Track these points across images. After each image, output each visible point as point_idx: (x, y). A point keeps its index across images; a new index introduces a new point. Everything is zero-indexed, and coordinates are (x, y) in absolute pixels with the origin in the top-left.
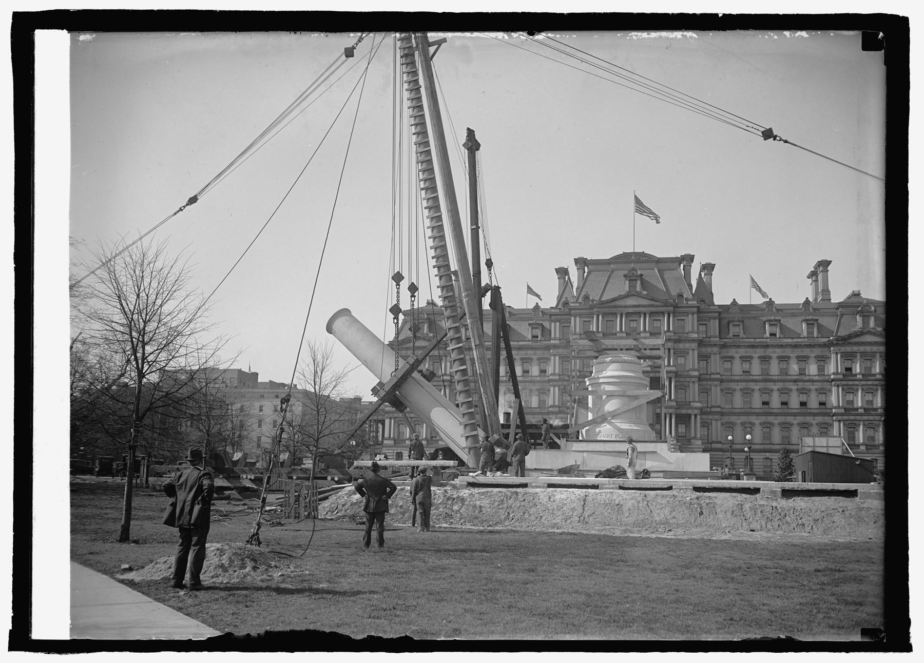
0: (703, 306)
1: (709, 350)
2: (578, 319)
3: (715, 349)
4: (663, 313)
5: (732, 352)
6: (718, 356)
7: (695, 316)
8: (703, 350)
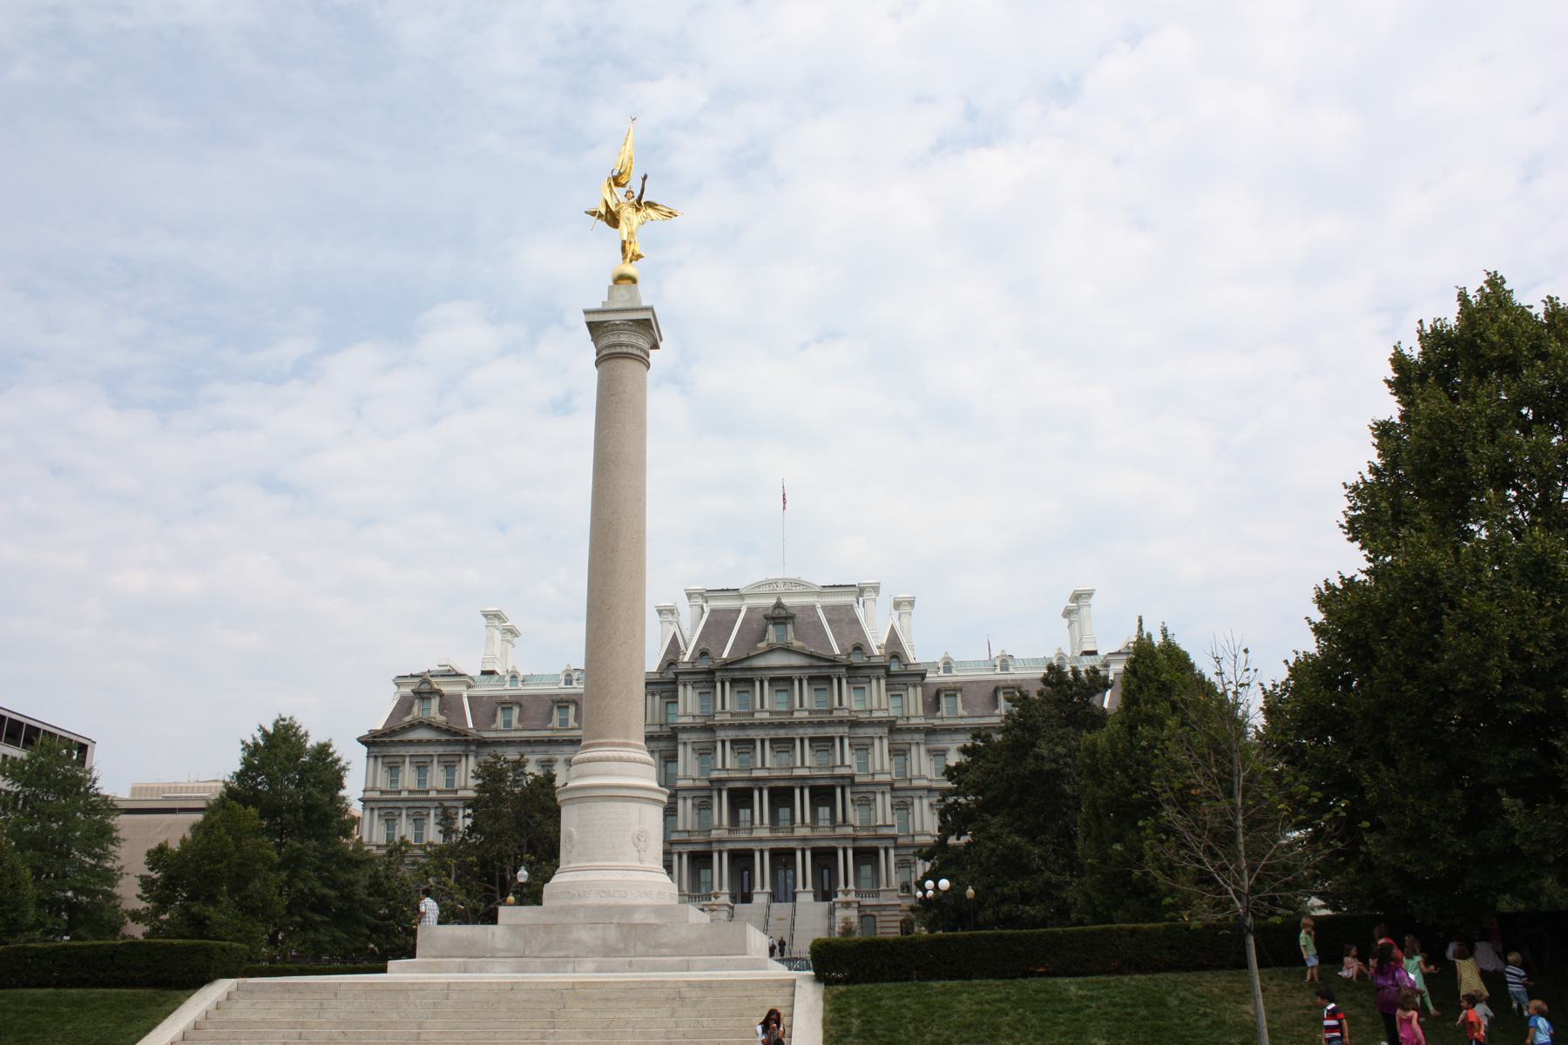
0: (894, 667)
1: (907, 738)
2: (689, 688)
3: (919, 737)
4: (751, 682)
6: (923, 749)
7: (883, 682)
8: (898, 738)
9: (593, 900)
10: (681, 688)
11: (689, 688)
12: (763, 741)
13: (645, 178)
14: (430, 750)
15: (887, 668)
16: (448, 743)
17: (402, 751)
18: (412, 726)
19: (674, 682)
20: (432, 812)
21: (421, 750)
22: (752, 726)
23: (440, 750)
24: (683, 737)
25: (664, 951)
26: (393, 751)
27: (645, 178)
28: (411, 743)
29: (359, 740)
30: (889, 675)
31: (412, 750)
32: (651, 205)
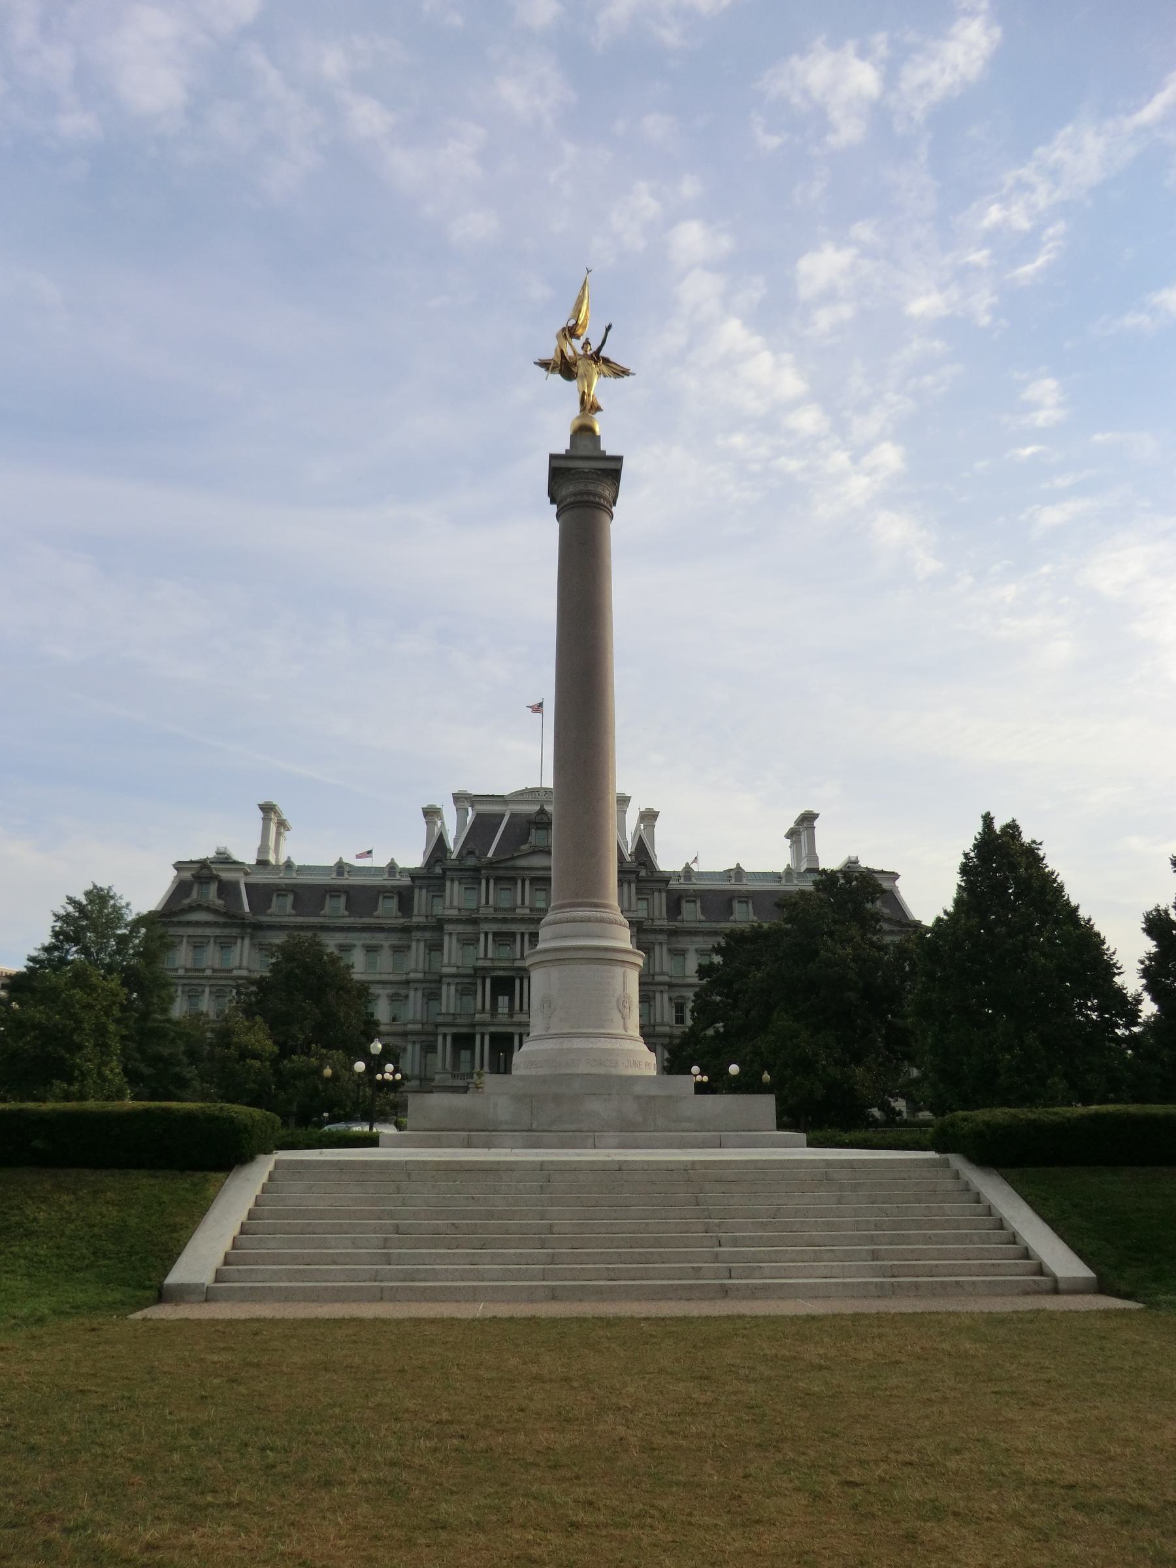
1: (652, 937)
2: (456, 883)
3: (662, 938)
4: (513, 880)
5: (683, 943)
6: (665, 948)
7: (633, 886)
9: (583, 1069)
10: (448, 884)
11: (456, 883)
12: (522, 934)
13: (608, 329)
14: (208, 931)
16: (225, 925)
17: (181, 931)
18: (192, 909)
19: (443, 877)
20: (207, 990)
21: (199, 931)
22: (514, 920)
23: (218, 931)
24: (448, 927)
25: (687, 1125)
27: (608, 329)
28: (189, 924)
29: (817, 815)
30: (639, 880)
31: (191, 931)
32: (606, 361)
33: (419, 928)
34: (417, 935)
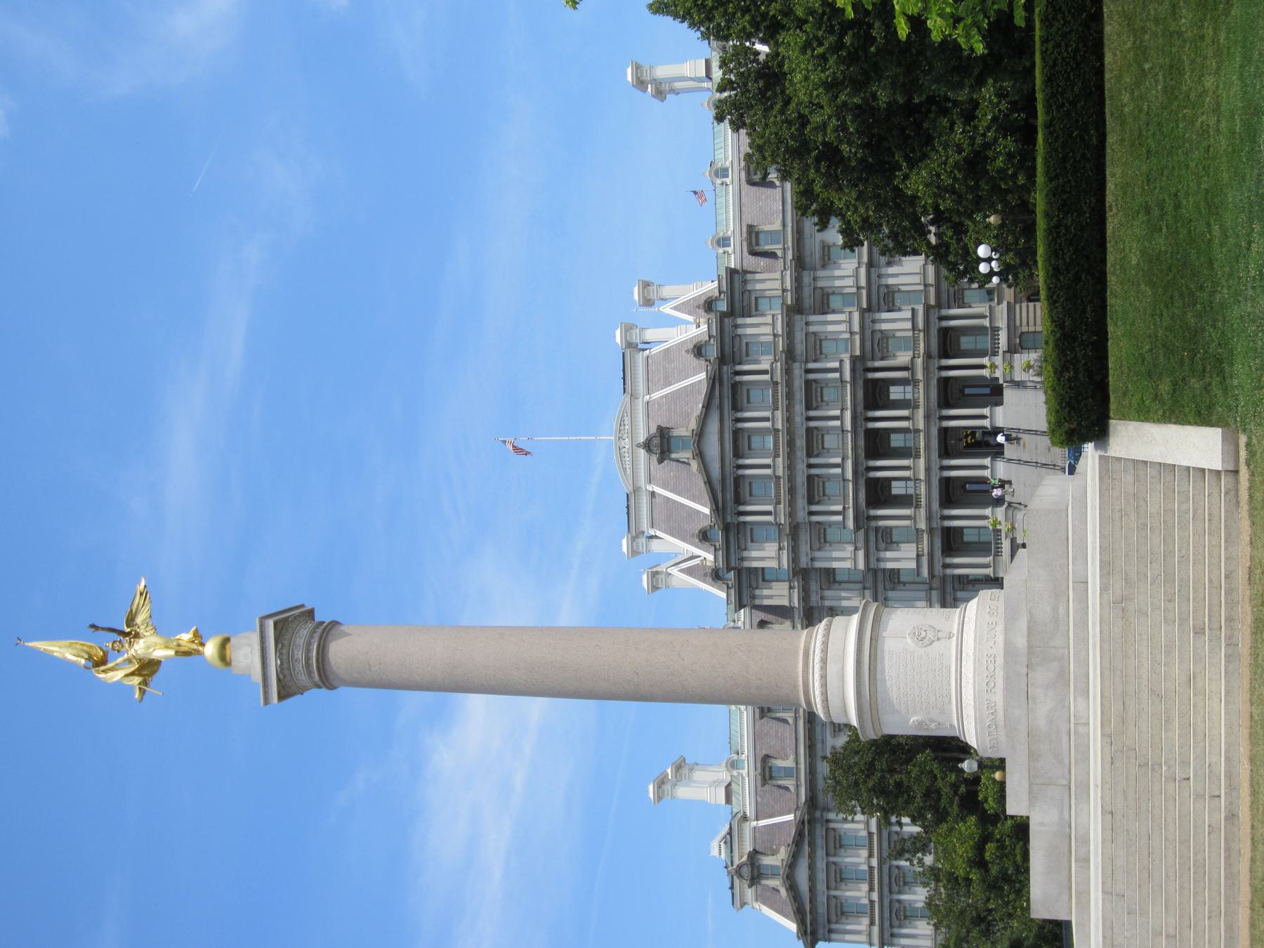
1: (807, 291)
2: (745, 554)
3: (807, 279)
6: (820, 273)
7: (740, 321)
8: (808, 302)
10: (746, 564)
11: (745, 554)
14: (821, 864)
15: (723, 315)
16: (812, 845)
17: (822, 899)
21: (821, 876)
23: (820, 853)
26: (822, 909)
28: (812, 890)
31: (821, 886)
33: (805, 597)
34: (814, 600)
